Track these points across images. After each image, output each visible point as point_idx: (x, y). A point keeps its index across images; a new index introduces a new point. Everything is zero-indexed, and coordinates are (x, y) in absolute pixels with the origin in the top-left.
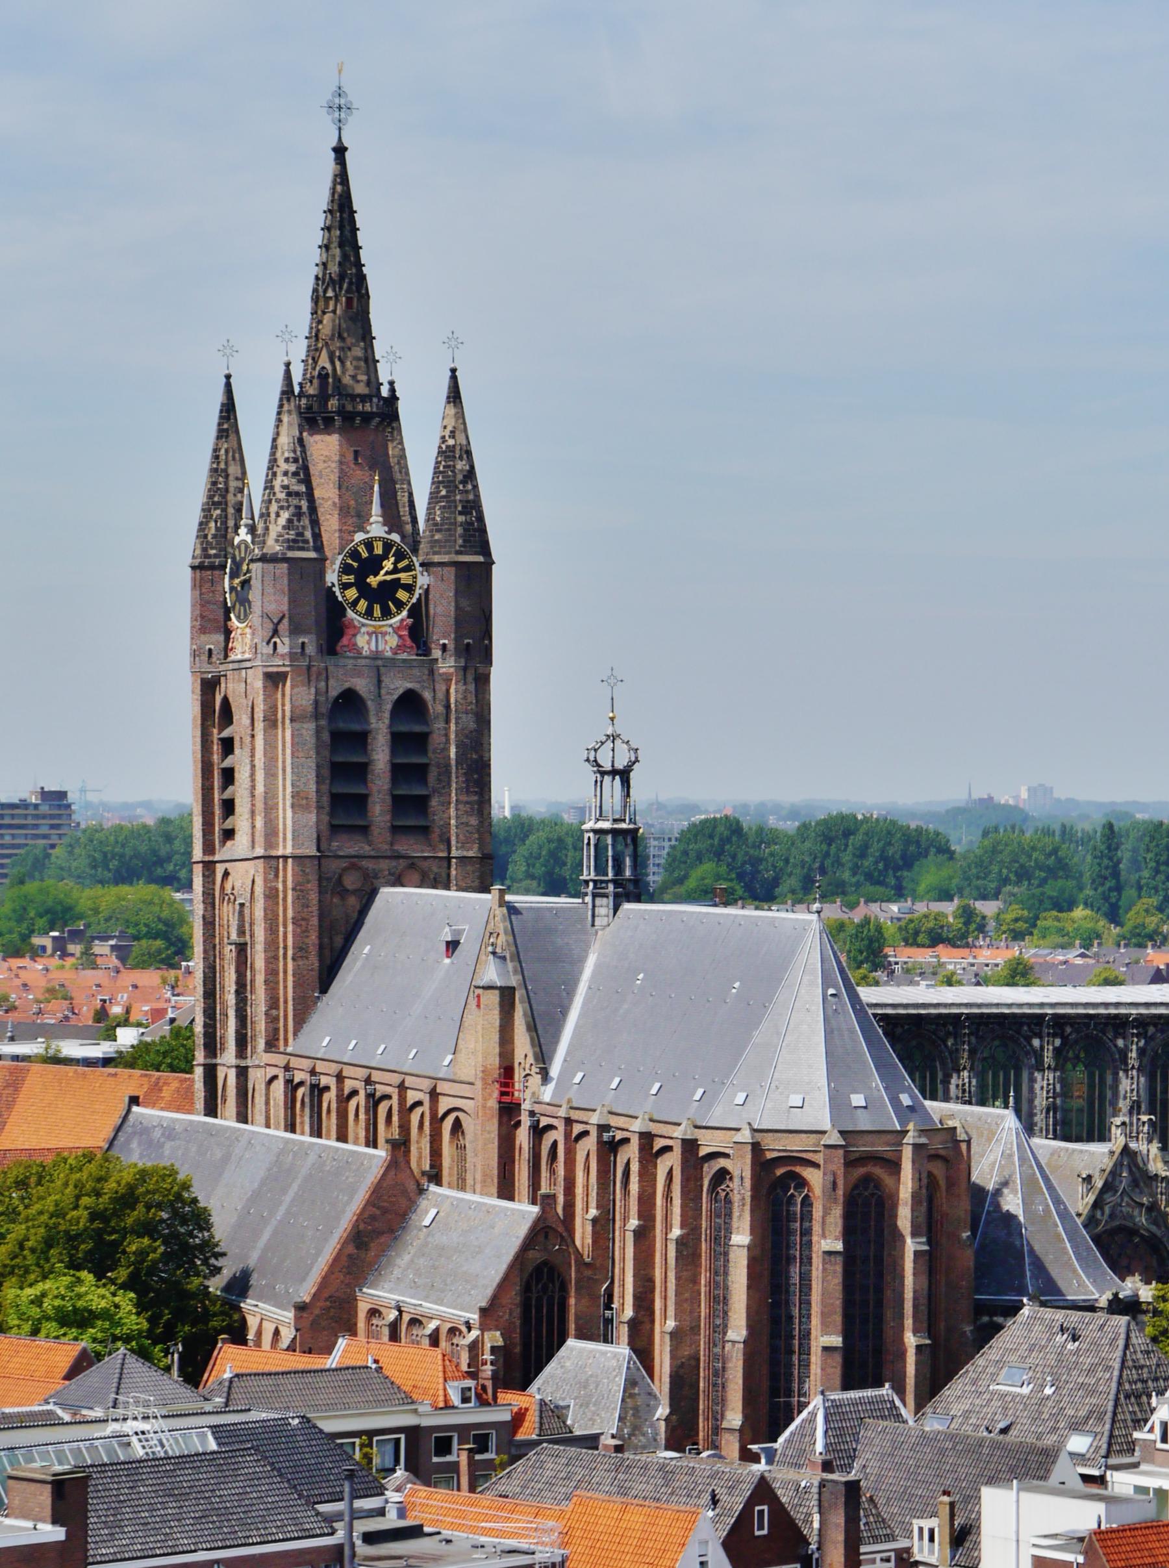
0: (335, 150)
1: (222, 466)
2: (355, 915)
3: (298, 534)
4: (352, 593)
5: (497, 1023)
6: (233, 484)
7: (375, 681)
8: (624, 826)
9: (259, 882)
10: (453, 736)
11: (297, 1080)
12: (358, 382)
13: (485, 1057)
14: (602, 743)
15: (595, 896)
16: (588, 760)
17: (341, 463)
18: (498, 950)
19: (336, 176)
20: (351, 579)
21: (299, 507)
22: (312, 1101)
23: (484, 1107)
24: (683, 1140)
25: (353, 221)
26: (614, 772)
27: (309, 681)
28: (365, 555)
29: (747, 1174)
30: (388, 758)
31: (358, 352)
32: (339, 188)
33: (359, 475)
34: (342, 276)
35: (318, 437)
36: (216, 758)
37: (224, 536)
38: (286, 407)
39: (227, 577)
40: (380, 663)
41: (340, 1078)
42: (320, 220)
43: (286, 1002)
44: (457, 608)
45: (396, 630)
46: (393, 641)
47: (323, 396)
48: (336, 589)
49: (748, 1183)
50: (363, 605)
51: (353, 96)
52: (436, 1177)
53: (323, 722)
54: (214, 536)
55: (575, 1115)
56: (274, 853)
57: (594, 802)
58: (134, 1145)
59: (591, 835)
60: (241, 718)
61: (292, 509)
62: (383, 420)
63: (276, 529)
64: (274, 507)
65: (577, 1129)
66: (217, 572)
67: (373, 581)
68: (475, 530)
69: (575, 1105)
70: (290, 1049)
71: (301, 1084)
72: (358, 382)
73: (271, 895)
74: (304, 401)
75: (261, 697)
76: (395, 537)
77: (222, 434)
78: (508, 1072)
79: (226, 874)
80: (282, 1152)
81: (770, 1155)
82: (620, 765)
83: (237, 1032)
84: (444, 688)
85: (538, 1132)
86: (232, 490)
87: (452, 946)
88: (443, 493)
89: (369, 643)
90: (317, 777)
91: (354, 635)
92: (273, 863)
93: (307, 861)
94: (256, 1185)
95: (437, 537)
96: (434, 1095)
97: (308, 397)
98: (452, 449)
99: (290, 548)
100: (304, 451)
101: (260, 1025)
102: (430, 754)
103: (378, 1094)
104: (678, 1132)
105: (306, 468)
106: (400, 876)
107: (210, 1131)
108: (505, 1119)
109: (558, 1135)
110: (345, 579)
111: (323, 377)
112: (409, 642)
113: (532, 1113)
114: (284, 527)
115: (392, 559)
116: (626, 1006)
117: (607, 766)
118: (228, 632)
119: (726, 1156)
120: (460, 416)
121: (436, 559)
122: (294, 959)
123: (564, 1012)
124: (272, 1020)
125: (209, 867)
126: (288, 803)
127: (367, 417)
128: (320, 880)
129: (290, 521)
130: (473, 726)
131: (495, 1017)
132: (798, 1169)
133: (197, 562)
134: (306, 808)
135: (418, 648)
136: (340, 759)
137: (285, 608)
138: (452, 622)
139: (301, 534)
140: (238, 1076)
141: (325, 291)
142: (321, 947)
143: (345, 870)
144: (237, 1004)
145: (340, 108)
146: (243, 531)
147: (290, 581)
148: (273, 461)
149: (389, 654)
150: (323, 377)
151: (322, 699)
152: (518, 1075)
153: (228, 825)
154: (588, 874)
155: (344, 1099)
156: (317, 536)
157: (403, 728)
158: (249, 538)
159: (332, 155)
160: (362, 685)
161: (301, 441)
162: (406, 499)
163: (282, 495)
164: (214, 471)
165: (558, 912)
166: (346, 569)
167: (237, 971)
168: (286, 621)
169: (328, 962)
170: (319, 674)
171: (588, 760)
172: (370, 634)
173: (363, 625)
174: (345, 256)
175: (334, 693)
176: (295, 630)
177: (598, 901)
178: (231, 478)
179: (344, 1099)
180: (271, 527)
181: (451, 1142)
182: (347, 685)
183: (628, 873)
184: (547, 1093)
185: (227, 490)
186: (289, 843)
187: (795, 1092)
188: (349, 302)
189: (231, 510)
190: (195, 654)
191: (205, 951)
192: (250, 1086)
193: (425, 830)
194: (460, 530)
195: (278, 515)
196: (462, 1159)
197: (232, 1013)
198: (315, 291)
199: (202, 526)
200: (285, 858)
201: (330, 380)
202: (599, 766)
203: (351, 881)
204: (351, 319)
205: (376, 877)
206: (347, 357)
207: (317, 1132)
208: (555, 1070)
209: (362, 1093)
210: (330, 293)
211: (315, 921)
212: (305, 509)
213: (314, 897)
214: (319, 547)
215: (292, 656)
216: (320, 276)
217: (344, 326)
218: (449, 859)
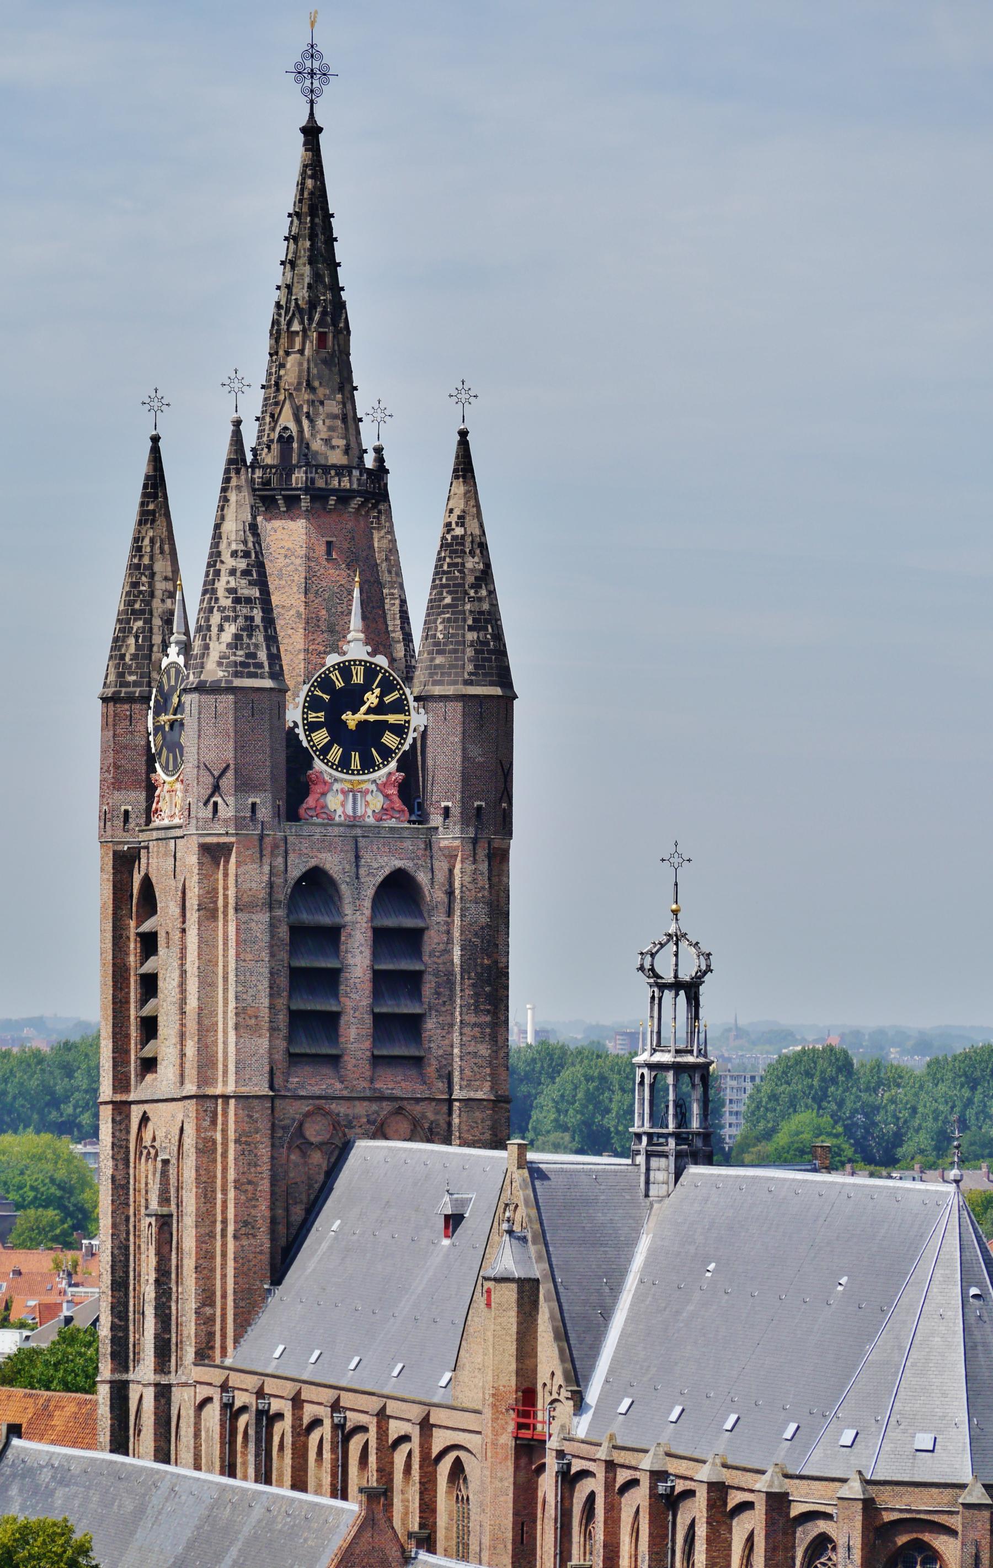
0: (304, 130)
1: (146, 561)
2: (321, 1178)
3: (248, 656)
4: (321, 737)
5: (514, 1329)
6: (160, 586)
7: (351, 856)
8: (690, 1059)
9: (190, 1131)
10: (457, 934)
11: (238, 1404)
12: (333, 447)
13: (496, 1377)
14: (662, 945)
15: (649, 1155)
16: (641, 968)
17: (308, 558)
18: (517, 1228)
19: (305, 166)
20: (320, 716)
21: (252, 619)
22: (258, 1433)
23: (494, 1444)
24: (768, 1494)
25: (328, 228)
26: (677, 985)
27: (261, 856)
28: (340, 684)
29: (857, 1542)
30: (367, 962)
31: (333, 407)
32: (309, 183)
33: (334, 575)
34: (313, 304)
35: (277, 523)
36: (132, 960)
37: (146, 655)
38: (234, 482)
39: (151, 713)
40: (359, 832)
41: (297, 1402)
42: (283, 226)
43: (224, 1296)
44: (465, 758)
45: (381, 788)
46: (377, 802)
47: (286, 468)
48: (300, 731)
49: (857, 1555)
50: (336, 753)
51: (331, 57)
52: (428, 1542)
53: (280, 913)
54: (135, 657)
55: (620, 1457)
56: (210, 1091)
57: (649, 1026)
58: (14, 1491)
59: (646, 1071)
60: (167, 905)
61: (241, 621)
62: (367, 500)
63: (218, 647)
64: (216, 619)
65: (623, 1476)
66: (137, 707)
67: (351, 719)
68: (490, 652)
69: (620, 1443)
70: (228, 1362)
71: (244, 1409)
72: (333, 447)
73: (206, 1149)
74: (258, 473)
75: (196, 878)
77: (146, 517)
78: (528, 1396)
79: (145, 1119)
80: (216, 1504)
81: (888, 1517)
82: (686, 974)
83: (157, 1337)
84: (445, 866)
85: (569, 1480)
86: (158, 593)
87: (453, 1222)
88: (448, 600)
89: (343, 805)
90: (271, 987)
91: (324, 794)
92: (209, 1104)
93: (256, 1102)
94: (180, 1549)
95: (439, 660)
96: (426, 1426)
97: (265, 467)
98: (460, 540)
99: (237, 675)
100: (258, 542)
101: (190, 1328)
102: (426, 958)
103: (349, 1425)
104: (762, 1483)
105: (261, 566)
106: (382, 1125)
107: (118, 1475)
108: (523, 1462)
109: (595, 1485)
110: (312, 716)
111: (285, 441)
112: (398, 804)
113: (560, 1454)
114: (229, 645)
115: (377, 691)
116: (690, 1308)
117: (669, 977)
118: (151, 789)
119: (828, 1516)
120: (472, 495)
121: (437, 690)
122: (235, 1237)
123: (606, 1316)
124: (205, 1321)
125: (121, 1109)
126: (231, 1023)
127: (344, 497)
128: (273, 1125)
129: (237, 637)
130: (484, 920)
131: (511, 1319)
132: (927, 1537)
133: (110, 692)
134: (254, 1030)
135: (411, 812)
136: (303, 963)
137: (230, 755)
138: (458, 777)
139: (254, 656)
140: (157, 1398)
141: (289, 324)
142: (273, 1221)
143: (308, 1115)
144: (157, 1298)
145: (312, 74)
146: (173, 650)
147: (236, 719)
148: (215, 556)
149: (371, 820)
150: (285, 441)
151: (279, 881)
152: (542, 1400)
153: (148, 1052)
154: (642, 1124)
155: (303, 1431)
156: (275, 658)
157: (390, 922)
158: (181, 660)
159: (301, 137)
160: (334, 863)
161: (254, 527)
162: (396, 609)
163: (226, 602)
164: (134, 568)
165: (597, 1177)
166: (313, 703)
167: (158, 1253)
168: (230, 774)
169: (283, 1242)
170: (275, 846)
171: (641, 968)
172: (343, 792)
173: (336, 780)
174: (317, 276)
175: (295, 873)
176: (244, 785)
177: (655, 1162)
178: (157, 577)
179: (303, 1431)
180: (212, 645)
181: (449, 1492)
182: (313, 863)
183: (695, 1124)
184: (582, 1426)
185: (152, 595)
186: (232, 1078)
187: (924, 1430)
188: (322, 337)
189: (157, 622)
190: (105, 818)
191: (114, 1226)
192: (174, 1413)
193: (418, 1062)
194: (470, 652)
195: (221, 629)
196: (465, 1516)
197: (150, 1311)
198: (275, 323)
199: (118, 642)
200: (226, 1098)
201: (295, 445)
202: (657, 976)
203: (316, 1131)
204: (325, 362)
205: (350, 1126)
206: (317, 414)
207: (265, 1476)
208: (592, 1396)
209: (327, 1423)
210: (296, 327)
211: (265, 1185)
212: (258, 620)
213: (264, 1151)
214: (277, 674)
215: (239, 822)
216: (283, 303)
217: (314, 371)
218: (450, 1102)
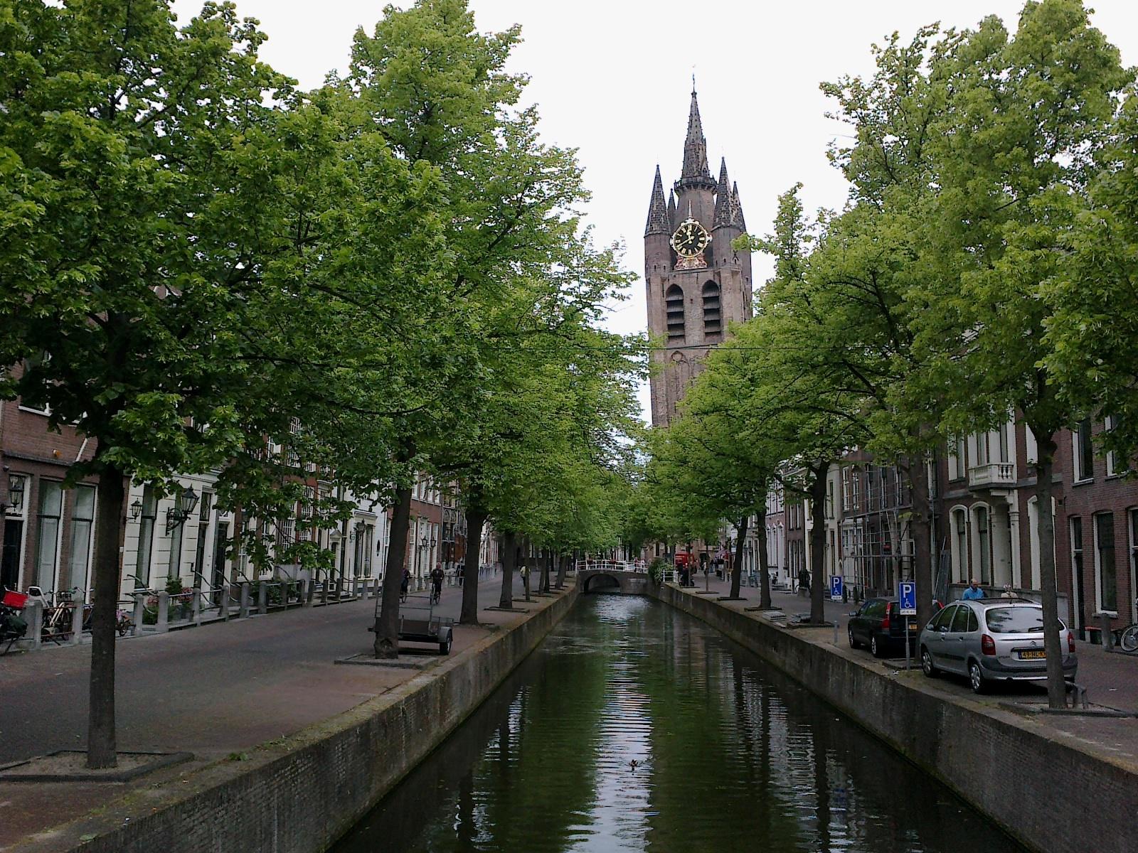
4: (679, 247)
50: (684, 250)
76: (697, 223)
112: (703, 262)
166: (677, 238)
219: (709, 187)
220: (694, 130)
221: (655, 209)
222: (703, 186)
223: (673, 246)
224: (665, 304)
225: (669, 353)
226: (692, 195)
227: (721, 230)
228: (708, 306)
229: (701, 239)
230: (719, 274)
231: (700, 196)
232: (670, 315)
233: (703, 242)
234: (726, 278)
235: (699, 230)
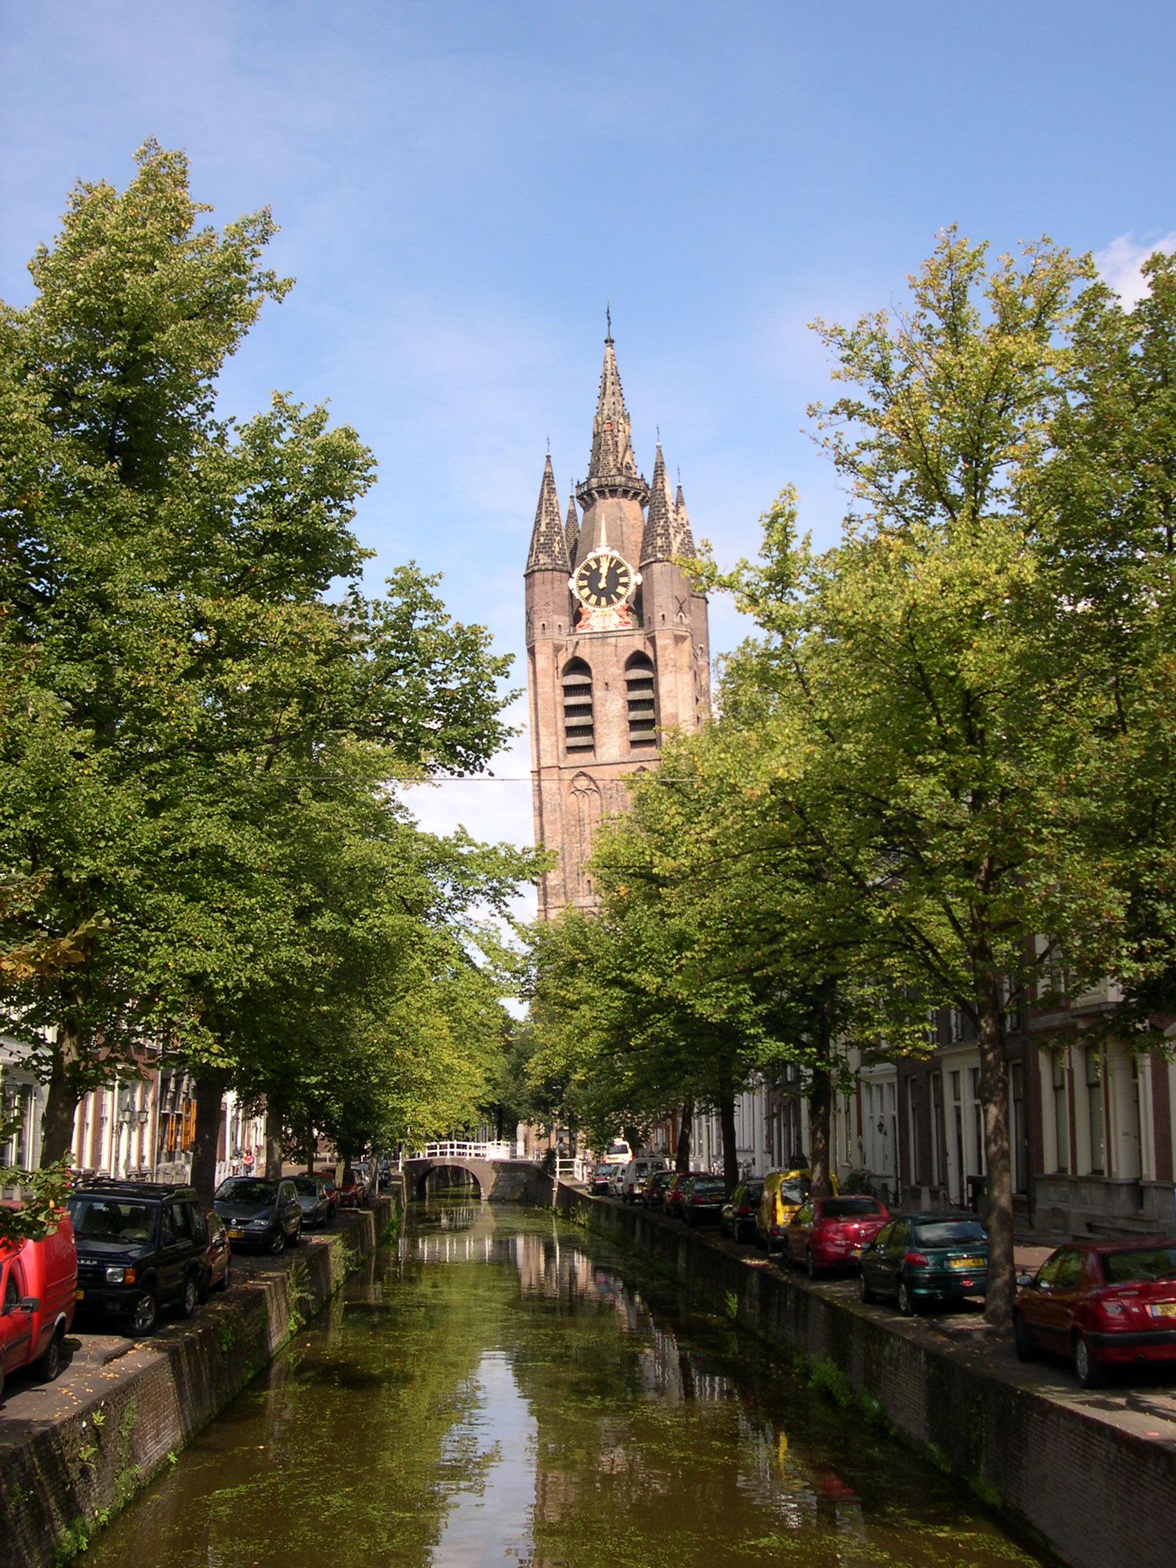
4: (586, 592)
20: (585, 583)
50: (594, 598)
76: (616, 554)
166: (582, 577)
219: (636, 495)
220: (609, 399)
221: (543, 528)
222: (625, 493)
223: (575, 592)
224: (560, 692)
225: (568, 775)
226: (605, 506)
227: (656, 567)
228: (637, 695)
229: (622, 580)
230: (652, 641)
231: (621, 509)
232: (570, 710)
233: (625, 585)
234: (665, 648)
235: (619, 565)
